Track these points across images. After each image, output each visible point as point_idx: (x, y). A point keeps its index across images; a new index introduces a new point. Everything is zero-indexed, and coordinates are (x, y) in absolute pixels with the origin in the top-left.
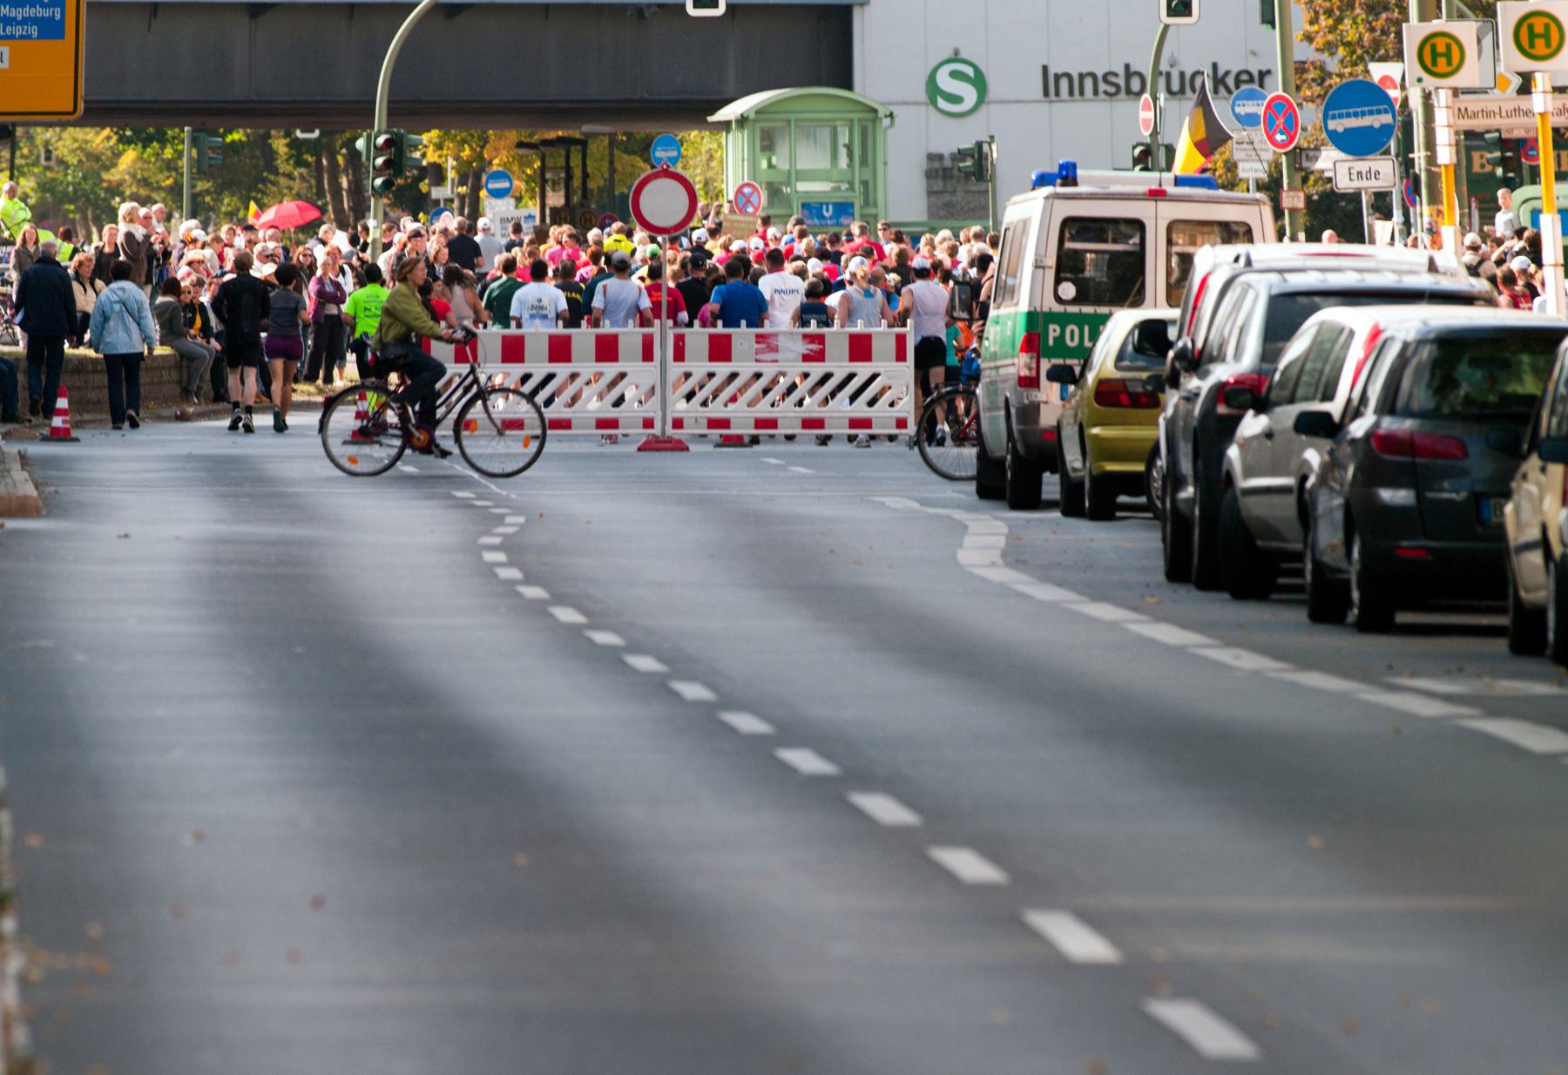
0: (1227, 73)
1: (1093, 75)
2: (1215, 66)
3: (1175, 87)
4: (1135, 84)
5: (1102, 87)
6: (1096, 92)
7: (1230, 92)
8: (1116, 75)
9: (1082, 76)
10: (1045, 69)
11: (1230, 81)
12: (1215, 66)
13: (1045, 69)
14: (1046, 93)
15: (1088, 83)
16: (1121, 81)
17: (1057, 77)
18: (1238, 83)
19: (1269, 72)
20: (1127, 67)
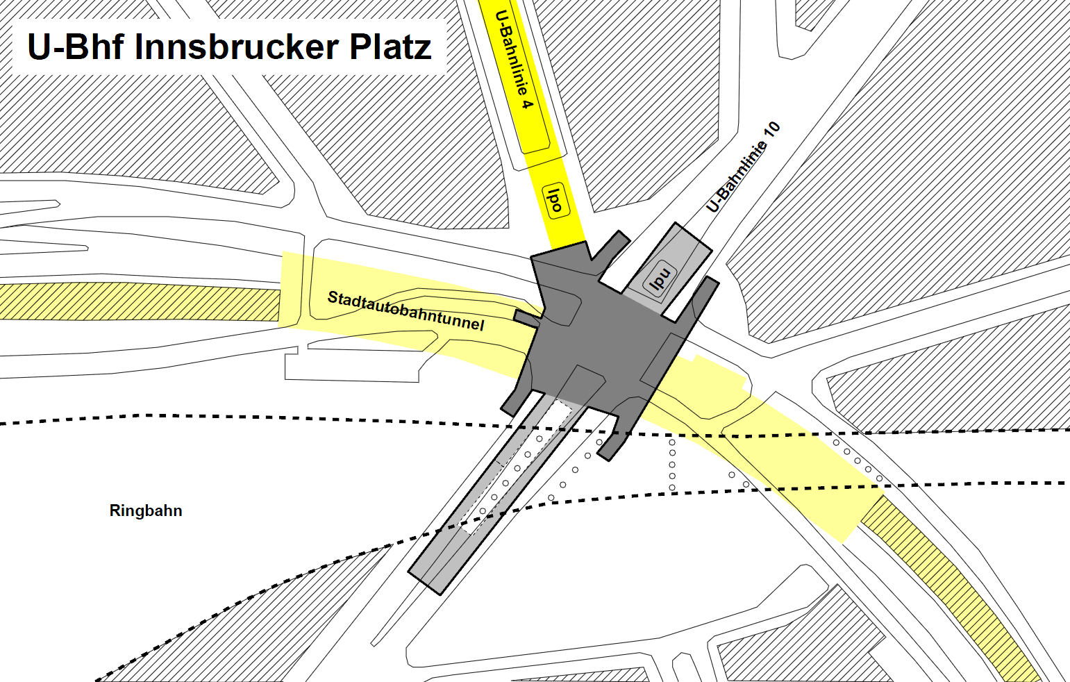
0: (299, 42)
1: (182, 43)
2: (290, 36)
3: (254, 51)
4: (219, 49)
5: (188, 50)
6: (183, 56)
7: (300, 57)
8: (202, 43)
9: (382, 310)
10: (139, 36)
11: (302, 48)
12: (290, 36)
13: (139, 36)
14: (139, 56)
15: (177, 47)
16: (207, 47)
17: (149, 44)
18: (309, 49)
19: (336, 42)
20: (212, 36)
